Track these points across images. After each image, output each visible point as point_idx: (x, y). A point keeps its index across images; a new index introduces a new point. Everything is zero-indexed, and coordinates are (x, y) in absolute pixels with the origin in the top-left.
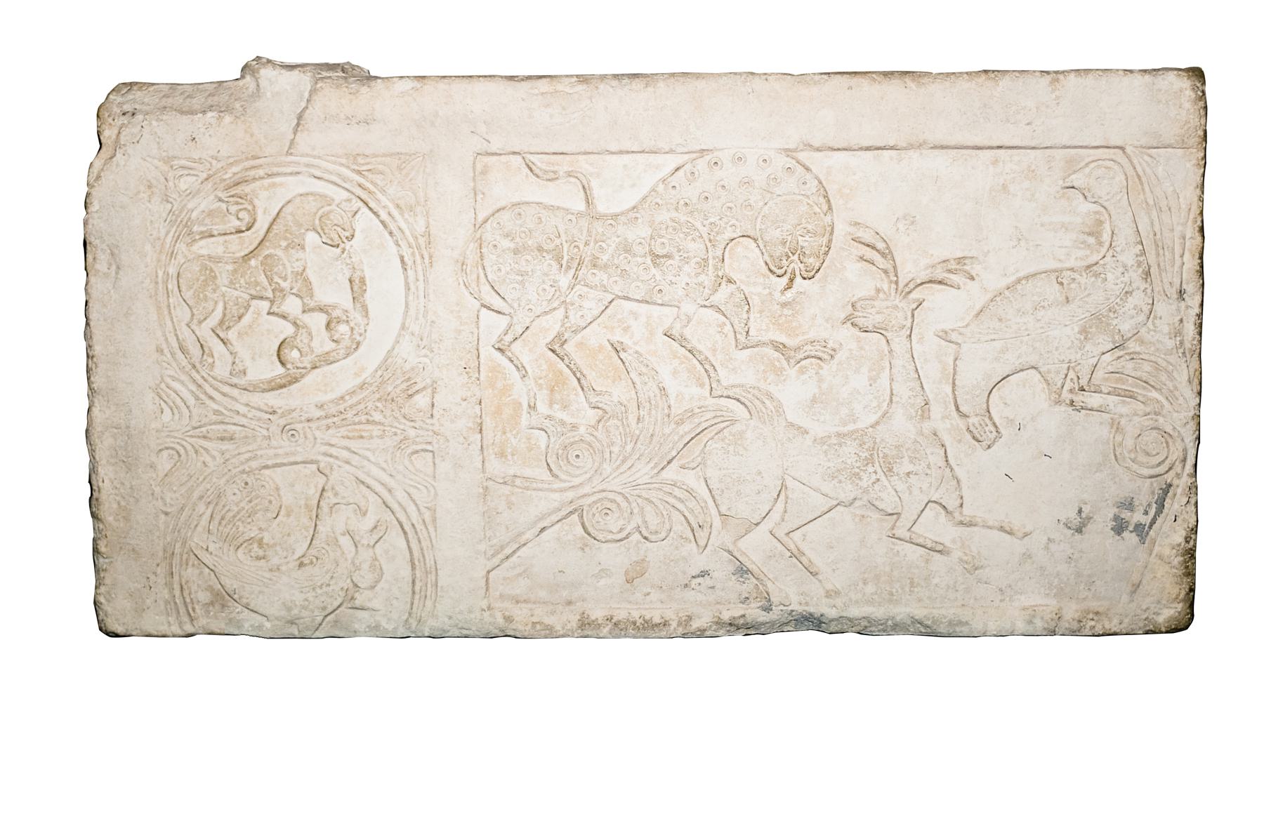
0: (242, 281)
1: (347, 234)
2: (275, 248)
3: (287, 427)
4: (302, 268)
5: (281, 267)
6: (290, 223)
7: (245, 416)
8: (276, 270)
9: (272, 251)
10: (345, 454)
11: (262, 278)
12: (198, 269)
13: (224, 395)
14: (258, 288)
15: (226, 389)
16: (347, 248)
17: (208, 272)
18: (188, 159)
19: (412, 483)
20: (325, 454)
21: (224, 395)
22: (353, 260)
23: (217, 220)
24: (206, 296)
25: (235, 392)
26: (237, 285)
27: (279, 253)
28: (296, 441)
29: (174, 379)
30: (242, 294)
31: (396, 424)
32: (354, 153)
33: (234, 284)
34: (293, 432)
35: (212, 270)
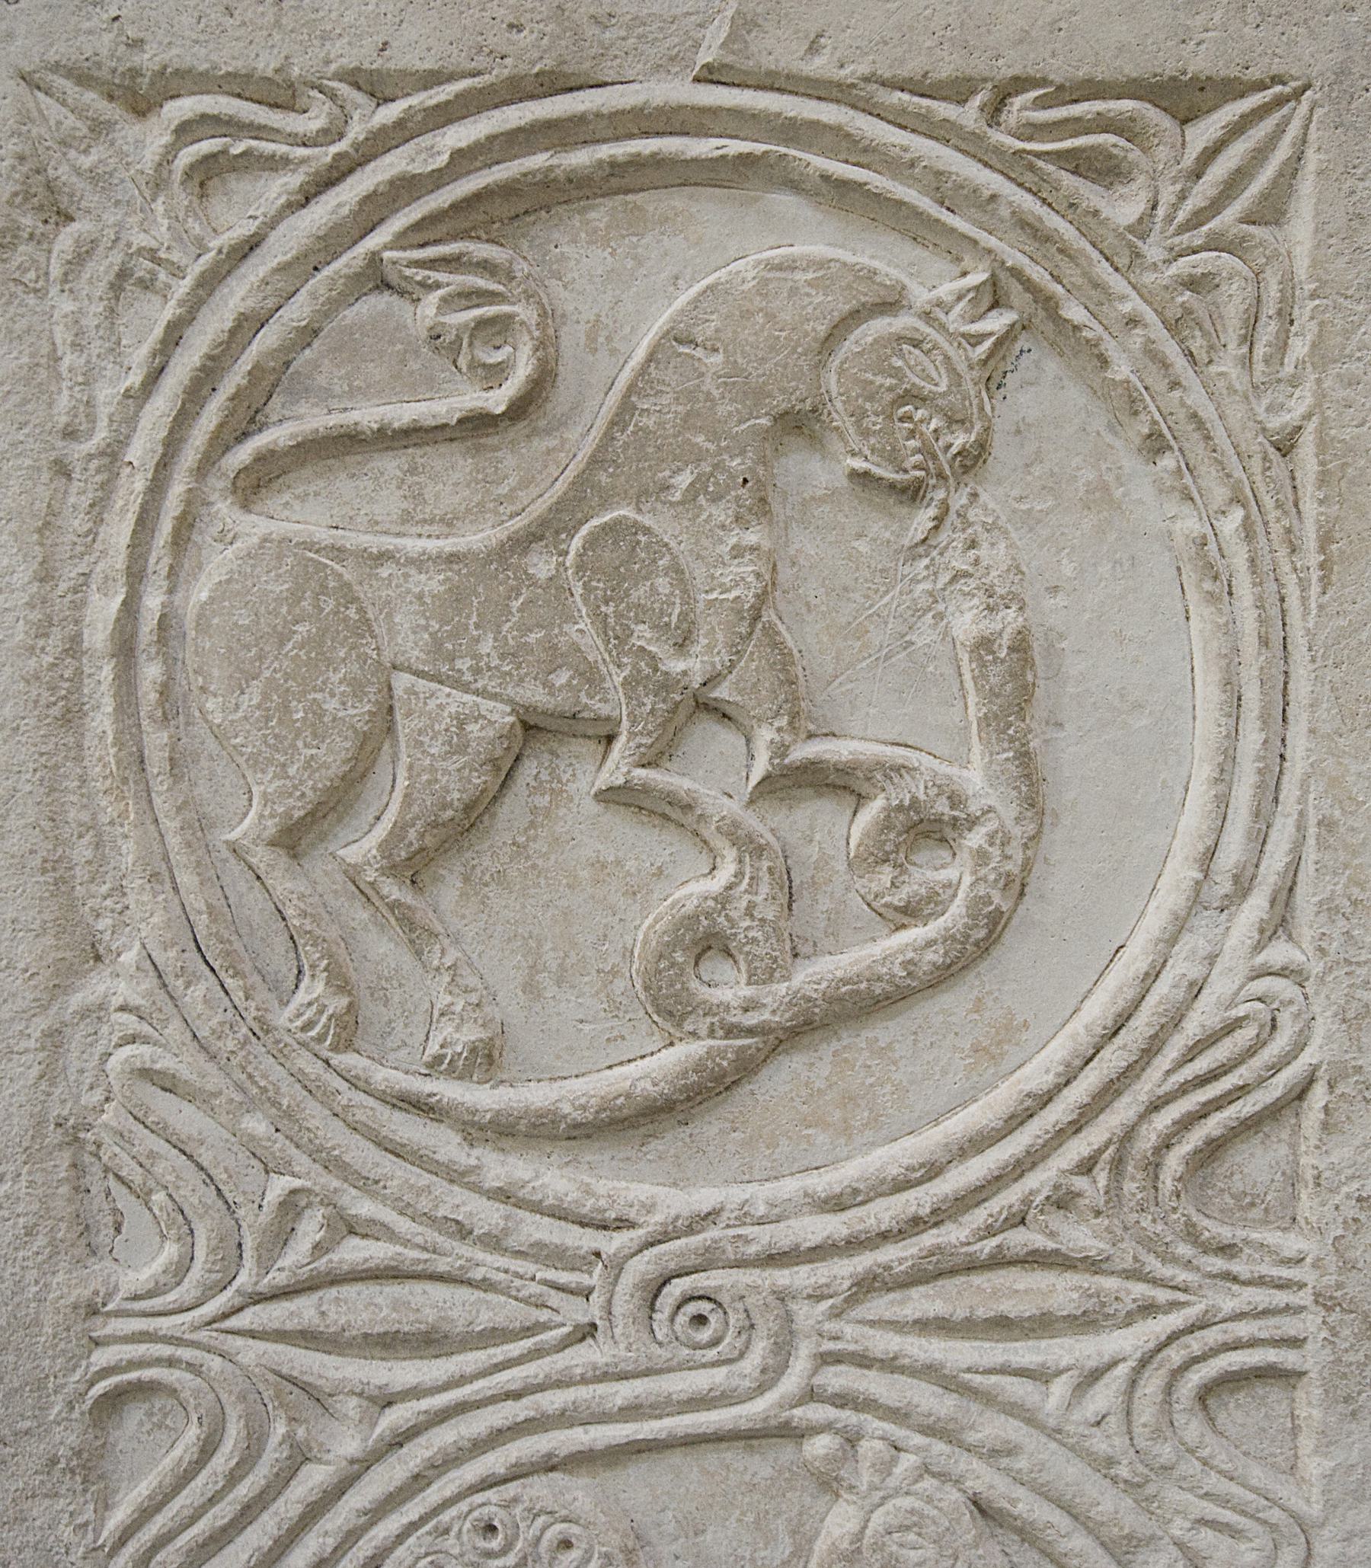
0: (486, 646)
1: (960, 440)
2: (640, 498)
3: (677, 1288)
4: (756, 586)
5: (663, 584)
6: (709, 385)
7: (493, 1242)
8: (639, 594)
9: (626, 512)
10: (928, 1399)
11: (582, 632)
12: (281, 588)
13: (396, 1151)
14: (562, 678)
15: (407, 1128)
16: (958, 500)
17: (329, 605)
18: (240, 84)
19: (1212, 1510)
20: (841, 1400)
21: (396, 1151)
22: (983, 552)
23: (376, 372)
24: (317, 711)
25: (445, 1142)
26: (464, 664)
27: (659, 522)
28: (715, 1342)
29: (168, 1084)
30: (486, 705)
31: (1153, 1264)
32: (1006, 70)
33: (452, 658)
34: (704, 1307)
35: (347, 595)
